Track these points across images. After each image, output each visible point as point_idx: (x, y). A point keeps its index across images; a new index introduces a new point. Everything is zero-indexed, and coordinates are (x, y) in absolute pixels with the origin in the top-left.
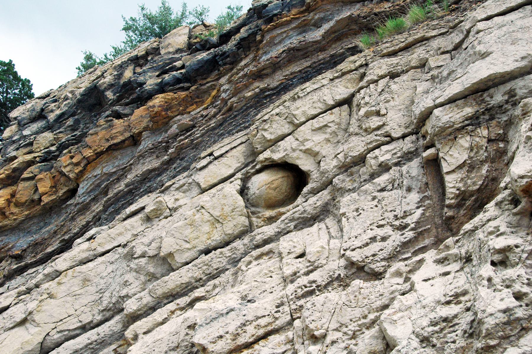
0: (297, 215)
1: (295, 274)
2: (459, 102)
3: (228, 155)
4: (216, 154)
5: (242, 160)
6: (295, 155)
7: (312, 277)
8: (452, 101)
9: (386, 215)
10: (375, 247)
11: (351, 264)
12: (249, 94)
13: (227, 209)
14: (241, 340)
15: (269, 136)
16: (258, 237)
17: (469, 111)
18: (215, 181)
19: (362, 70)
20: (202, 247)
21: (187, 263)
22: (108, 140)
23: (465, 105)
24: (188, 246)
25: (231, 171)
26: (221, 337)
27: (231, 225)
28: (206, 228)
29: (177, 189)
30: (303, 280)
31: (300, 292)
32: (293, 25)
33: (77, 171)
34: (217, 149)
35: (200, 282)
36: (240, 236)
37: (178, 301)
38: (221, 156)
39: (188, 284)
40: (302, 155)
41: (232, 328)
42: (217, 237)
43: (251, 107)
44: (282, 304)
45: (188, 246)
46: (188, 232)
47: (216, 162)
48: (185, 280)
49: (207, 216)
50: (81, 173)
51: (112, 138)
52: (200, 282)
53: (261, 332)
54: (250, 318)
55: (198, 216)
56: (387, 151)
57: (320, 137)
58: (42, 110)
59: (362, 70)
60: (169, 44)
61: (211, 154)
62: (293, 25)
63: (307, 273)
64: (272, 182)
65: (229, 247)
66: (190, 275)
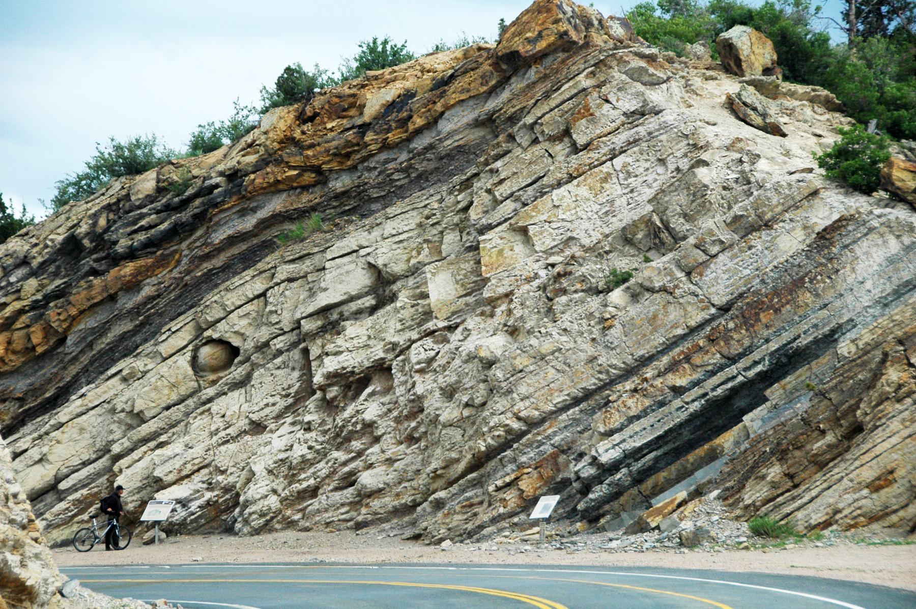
0: (229, 381)
1: (217, 430)
2: (315, 317)
3: (183, 330)
4: (173, 329)
5: (194, 333)
6: (227, 335)
7: (228, 431)
8: (310, 315)
9: (277, 387)
10: (267, 411)
11: (252, 422)
12: (200, 274)
13: (180, 377)
14: (184, 473)
15: (210, 319)
16: (203, 397)
17: (319, 323)
18: (173, 351)
19: (273, 271)
20: (164, 405)
21: (154, 417)
22: (89, 300)
23: (318, 319)
24: (153, 405)
25: (185, 343)
26: (171, 472)
27: (184, 388)
28: (166, 391)
29: (147, 355)
30: (222, 434)
31: (220, 442)
32: (234, 210)
33: (64, 327)
34: (174, 325)
35: (163, 431)
36: (191, 395)
37: (149, 444)
38: (177, 330)
39: (155, 432)
40: (232, 335)
41: (177, 466)
42: (174, 397)
43: (202, 282)
44: (209, 449)
45: (153, 405)
46: (153, 395)
47: (173, 336)
48: (153, 429)
49: (166, 383)
50: (69, 328)
51: (93, 299)
52: (163, 431)
53: (196, 467)
54: (189, 459)
55: (159, 383)
56: (281, 341)
57: (244, 322)
58: (26, 257)
59: (273, 271)
60: (139, 191)
61: (169, 330)
62: (234, 210)
63: (225, 429)
64: (213, 354)
65: (183, 404)
66: (156, 426)
